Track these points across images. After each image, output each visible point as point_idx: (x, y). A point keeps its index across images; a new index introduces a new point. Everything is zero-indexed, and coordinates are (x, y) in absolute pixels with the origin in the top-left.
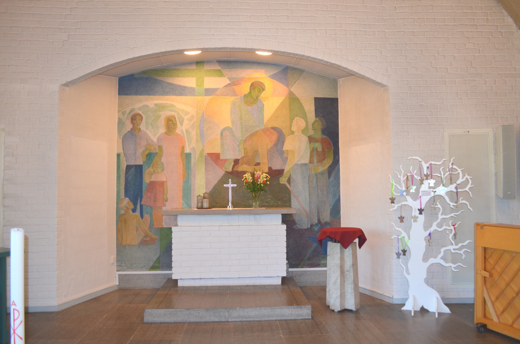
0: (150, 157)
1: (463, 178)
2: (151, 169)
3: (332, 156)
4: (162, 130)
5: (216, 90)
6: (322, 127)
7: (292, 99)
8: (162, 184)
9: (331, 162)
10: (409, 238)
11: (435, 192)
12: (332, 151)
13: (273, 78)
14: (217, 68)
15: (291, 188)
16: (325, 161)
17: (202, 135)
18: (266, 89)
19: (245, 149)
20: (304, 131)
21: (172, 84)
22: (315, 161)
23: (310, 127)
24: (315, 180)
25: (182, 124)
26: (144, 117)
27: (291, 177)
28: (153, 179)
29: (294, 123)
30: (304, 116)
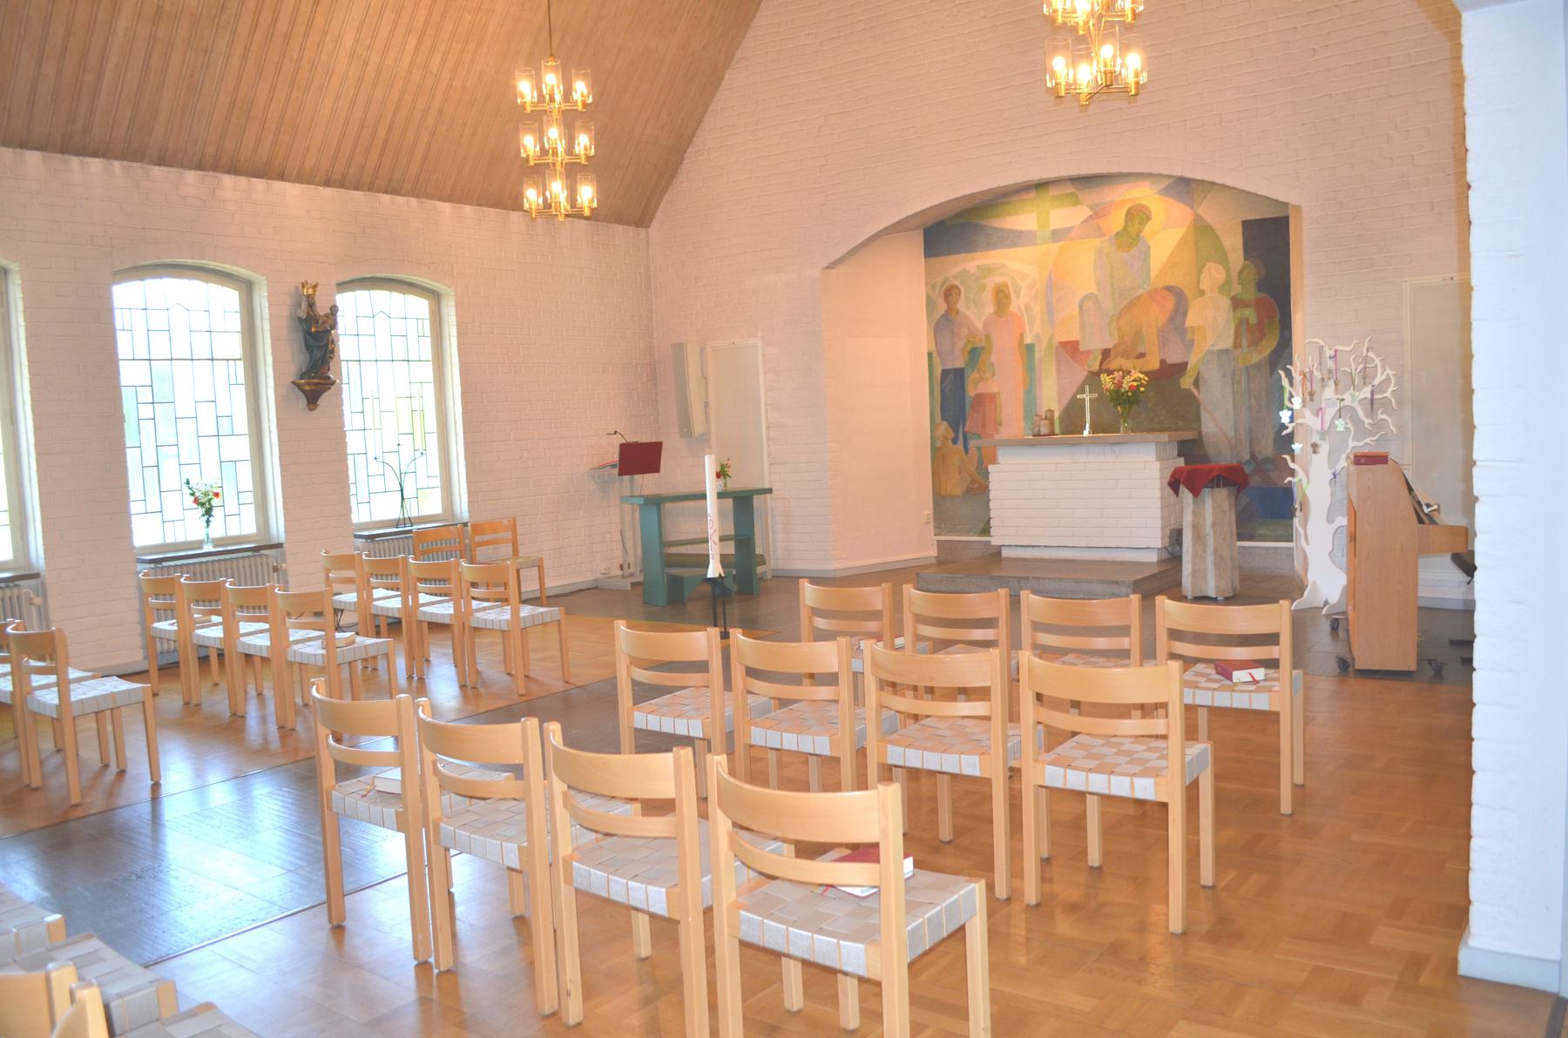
0: (974, 354)
1: (1382, 374)
2: (976, 375)
3: (1277, 332)
4: (990, 309)
5: (1069, 230)
6: (1257, 277)
7: (1201, 229)
8: (993, 397)
9: (1274, 344)
10: (1308, 482)
11: (1343, 400)
12: (1277, 323)
13: (1164, 195)
14: (1068, 192)
15: (1201, 396)
16: (1264, 343)
17: (1050, 312)
18: (1153, 218)
19: (1119, 330)
20: (1221, 289)
21: (1002, 230)
22: (1244, 342)
23: (1235, 278)
24: (1244, 379)
25: (1018, 295)
26: (962, 289)
27: (1200, 376)
28: (980, 389)
29: (1204, 275)
30: (1223, 259)
